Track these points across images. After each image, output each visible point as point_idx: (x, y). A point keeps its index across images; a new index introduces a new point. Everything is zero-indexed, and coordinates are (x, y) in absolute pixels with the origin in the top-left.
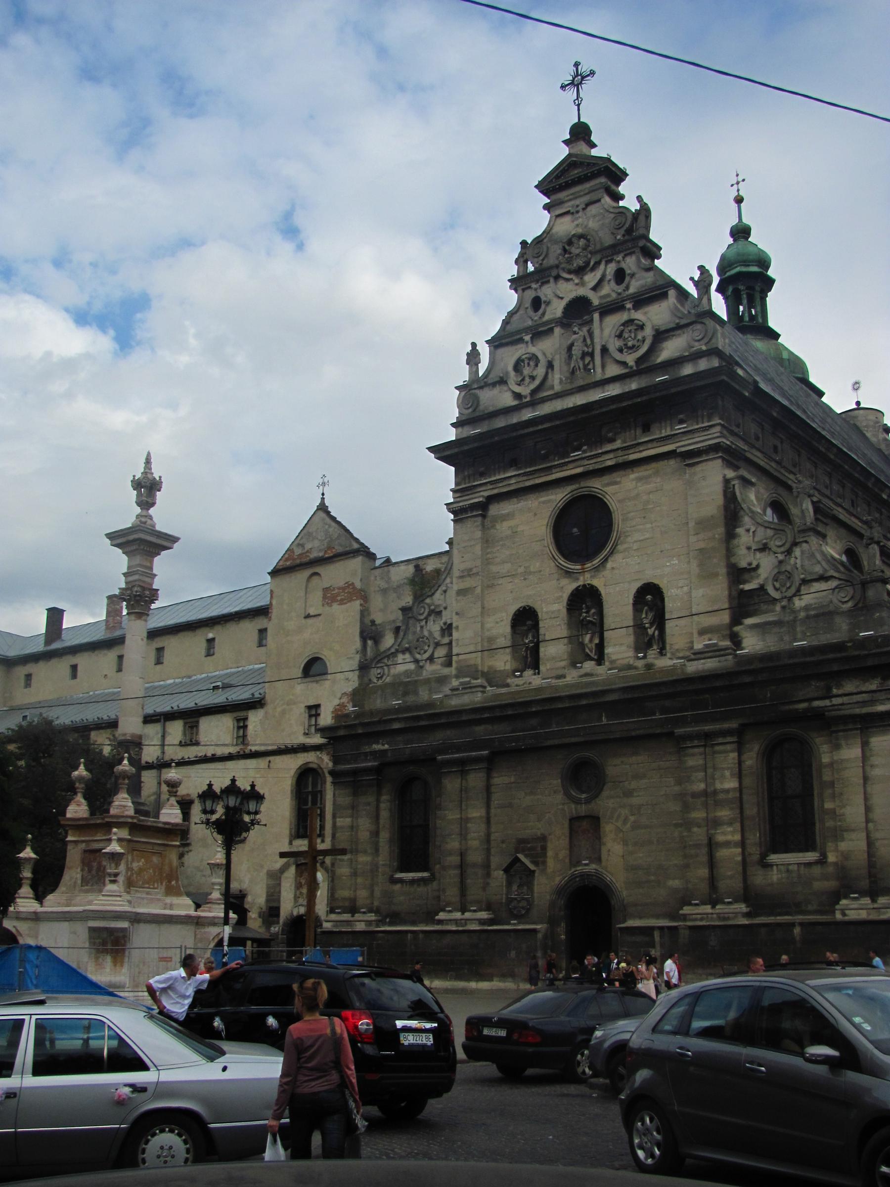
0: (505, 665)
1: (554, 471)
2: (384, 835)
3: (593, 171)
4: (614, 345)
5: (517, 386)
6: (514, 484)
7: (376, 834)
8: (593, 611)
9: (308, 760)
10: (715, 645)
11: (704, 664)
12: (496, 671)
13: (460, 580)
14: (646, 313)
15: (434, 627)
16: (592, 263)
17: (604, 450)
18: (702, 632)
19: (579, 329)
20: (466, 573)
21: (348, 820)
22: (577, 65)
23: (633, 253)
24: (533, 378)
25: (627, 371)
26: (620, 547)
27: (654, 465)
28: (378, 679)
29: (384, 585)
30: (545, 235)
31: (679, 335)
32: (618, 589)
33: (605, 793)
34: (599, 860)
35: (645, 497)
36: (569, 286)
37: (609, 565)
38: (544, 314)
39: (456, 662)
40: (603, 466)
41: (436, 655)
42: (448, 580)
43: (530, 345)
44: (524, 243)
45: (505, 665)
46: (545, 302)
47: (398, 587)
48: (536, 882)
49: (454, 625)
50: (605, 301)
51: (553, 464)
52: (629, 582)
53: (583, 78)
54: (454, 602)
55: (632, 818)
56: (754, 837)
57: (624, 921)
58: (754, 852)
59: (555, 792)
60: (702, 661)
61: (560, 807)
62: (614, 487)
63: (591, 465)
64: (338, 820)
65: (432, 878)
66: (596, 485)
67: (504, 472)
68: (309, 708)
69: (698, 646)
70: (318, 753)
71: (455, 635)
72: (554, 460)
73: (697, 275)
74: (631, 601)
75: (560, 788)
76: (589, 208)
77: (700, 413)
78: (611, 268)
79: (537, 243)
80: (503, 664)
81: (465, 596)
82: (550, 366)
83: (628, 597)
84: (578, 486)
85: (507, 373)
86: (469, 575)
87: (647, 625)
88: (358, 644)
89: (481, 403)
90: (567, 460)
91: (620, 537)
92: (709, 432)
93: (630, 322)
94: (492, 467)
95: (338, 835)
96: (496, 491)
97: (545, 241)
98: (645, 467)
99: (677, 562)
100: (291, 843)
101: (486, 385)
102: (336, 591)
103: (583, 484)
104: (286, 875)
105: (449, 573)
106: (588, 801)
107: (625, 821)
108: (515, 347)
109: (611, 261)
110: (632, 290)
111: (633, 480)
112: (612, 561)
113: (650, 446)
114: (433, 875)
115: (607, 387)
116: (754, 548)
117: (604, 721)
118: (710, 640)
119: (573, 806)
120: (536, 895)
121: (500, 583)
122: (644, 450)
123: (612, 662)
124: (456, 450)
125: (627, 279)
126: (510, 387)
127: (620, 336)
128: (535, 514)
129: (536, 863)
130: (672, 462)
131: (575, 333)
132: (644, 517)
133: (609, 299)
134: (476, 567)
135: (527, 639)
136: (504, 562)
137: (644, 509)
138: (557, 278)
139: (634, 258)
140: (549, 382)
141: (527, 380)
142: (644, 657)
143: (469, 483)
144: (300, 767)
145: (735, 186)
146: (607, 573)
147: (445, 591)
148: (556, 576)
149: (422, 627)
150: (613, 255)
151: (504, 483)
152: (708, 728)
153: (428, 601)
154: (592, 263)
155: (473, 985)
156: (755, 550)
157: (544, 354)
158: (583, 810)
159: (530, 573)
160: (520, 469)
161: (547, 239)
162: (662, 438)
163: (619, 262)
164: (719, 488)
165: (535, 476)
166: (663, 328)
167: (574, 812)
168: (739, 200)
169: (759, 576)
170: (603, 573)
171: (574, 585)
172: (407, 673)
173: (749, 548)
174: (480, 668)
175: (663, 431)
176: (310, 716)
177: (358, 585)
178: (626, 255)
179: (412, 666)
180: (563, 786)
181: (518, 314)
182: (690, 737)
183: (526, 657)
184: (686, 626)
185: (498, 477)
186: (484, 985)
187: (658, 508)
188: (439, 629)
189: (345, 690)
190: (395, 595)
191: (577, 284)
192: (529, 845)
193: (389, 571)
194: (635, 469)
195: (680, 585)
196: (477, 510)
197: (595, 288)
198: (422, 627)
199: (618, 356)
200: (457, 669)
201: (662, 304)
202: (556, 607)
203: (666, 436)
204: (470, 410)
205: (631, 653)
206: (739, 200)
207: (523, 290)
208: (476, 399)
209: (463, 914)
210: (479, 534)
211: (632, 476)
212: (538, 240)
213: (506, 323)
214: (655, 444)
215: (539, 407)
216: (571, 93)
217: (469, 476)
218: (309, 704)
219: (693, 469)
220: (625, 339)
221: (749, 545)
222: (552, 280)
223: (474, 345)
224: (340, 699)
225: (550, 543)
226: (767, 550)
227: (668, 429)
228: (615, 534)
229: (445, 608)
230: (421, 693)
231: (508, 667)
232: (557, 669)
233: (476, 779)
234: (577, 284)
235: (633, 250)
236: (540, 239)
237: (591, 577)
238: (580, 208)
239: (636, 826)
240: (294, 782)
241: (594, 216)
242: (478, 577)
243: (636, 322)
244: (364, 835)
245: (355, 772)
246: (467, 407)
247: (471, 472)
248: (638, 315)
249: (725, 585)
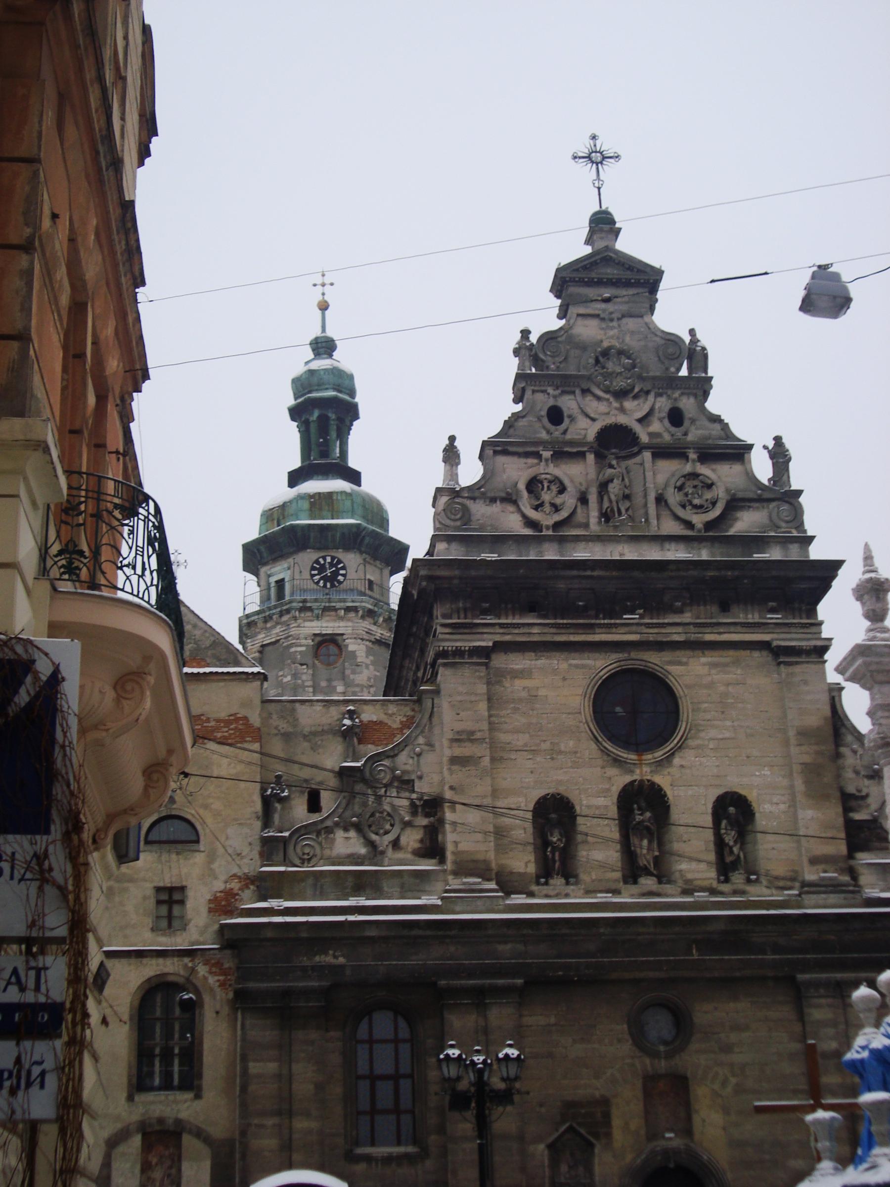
0: (526, 866)
1: (597, 630)
3: (639, 280)
4: (674, 499)
5: (533, 511)
6: (536, 634)
8: (648, 814)
9: (166, 970)
10: (830, 879)
11: (825, 899)
12: (512, 873)
13: (455, 744)
14: (713, 470)
16: (636, 390)
17: (671, 621)
18: (814, 861)
19: (617, 464)
20: (464, 737)
21: (272, 1067)
22: (594, 137)
23: (695, 396)
24: (556, 508)
25: (689, 533)
26: (690, 742)
27: (731, 653)
28: (303, 861)
29: (284, 726)
30: (562, 333)
31: (758, 508)
32: (690, 792)
33: (694, 1046)
34: (688, 1132)
35: (722, 688)
36: (602, 407)
37: (677, 761)
38: (565, 432)
39: (453, 853)
40: (668, 639)
41: (403, 840)
42: (421, 740)
43: (551, 465)
44: (525, 333)
45: (526, 866)
46: (570, 416)
47: (314, 734)
48: (596, 1160)
50: (655, 441)
51: (598, 621)
52: (706, 786)
53: (604, 158)
54: (446, 773)
55: (733, 1080)
59: (619, 1041)
60: (823, 896)
61: (628, 1061)
62: (677, 667)
63: (652, 635)
64: (251, 1065)
65: (425, 1153)
66: (654, 659)
67: (521, 617)
68: (158, 890)
69: (811, 875)
70: (186, 960)
71: (449, 816)
72: (597, 618)
73: (771, 444)
74: (710, 811)
75: (627, 1036)
76: (625, 321)
77: (796, 605)
78: (663, 404)
79: (552, 338)
80: (522, 865)
81: (464, 766)
82: (583, 500)
83: (705, 804)
84: (626, 655)
85: (518, 492)
86: (472, 741)
87: (731, 843)
88: (258, 806)
89: (472, 518)
90: (618, 621)
91: (690, 730)
92: (808, 631)
93: (694, 475)
94: (503, 606)
95: (252, 1088)
96: (507, 638)
97: (560, 339)
98: (721, 653)
99: (768, 773)
100: (130, 1098)
101: (483, 496)
102: (213, 724)
103: (633, 655)
104: (121, 1148)
105: (422, 732)
106: (669, 1056)
107: (724, 1083)
108: (523, 460)
109: (661, 395)
110: (690, 438)
111: (704, 665)
112: (681, 757)
113: (732, 629)
114: (425, 1153)
115: (667, 545)
116: (863, 773)
117: (695, 955)
118: (825, 872)
119: (648, 1061)
120: (597, 1179)
121: (513, 757)
122: (725, 633)
123: (688, 881)
124: (457, 573)
125: (686, 423)
126: (523, 508)
127: (680, 488)
128: (564, 679)
129: (597, 1136)
130: (756, 654)
131: (611, 466)
132: (723, 712)
133: (659, 440)
134: (480, 731)
135: (552, 835)
136: (517, 731)
137: (721, 702)
138: (586, 391)
139: (692, 400)
140: (580, 517)
141: (547, 508)
142: (727, 880)
143: (465, 618)
145: (319, 288)
146: (673, 770)
147: (419, 755)
148: (600, 762)
149: (378, 798)
150: (667, 389)
151: (522, 630)
152: (839, 976)
153: (386, 762)
154: (636, 390)
156: (863, 776)
157: (572, 481)
158: (662, 1065)
159: (560, 752)
160: (545, 617)
161: (564, 336)
162: (748, 623)
163: (676, 400)
164: (825, 698)
165: (572, 631)
166: (740, 495)
167: (649, 1068)
168: (324, 307)
169: (868, 806)
170: (669, 770)
171: (628, 779)
173: (857, 773)
174: (493, 865)
175: (750, 616)
176: (159, 902)
177: (255, 720)
178: (682, 394)
179: (363, 851)
180: (631, 1034)
181: (524, 420)
182: (817, 984)
183: (554, 861)
184: (785, 851)
185: (509, 621)
187: (740, 705)
189: (235, 870)
190: (306, 744)
191: (616, 409)
192: (583, 1111)
193: (294, 710)
194: (706, 652)
195: (775, 800)
196: (480, 657)
197: (640, 421)
198: (378, 798)
199: (681, 512)
200: (455, 862)
201: (733, 466)
202: (601, 801)
203: (755, 623)
204: (458, 523)
205: (712, 874)
206: (324, 307)
207: (534, 392)
208: (466, 510)
210: (482, 688)
211: (703, 660)
212: (548, 338)
213: (510, 424)
214: (739, 629)
215: (569, 546)
216: (587, 171)
217: (465, 610)
218: (161, 884)
219: (791, 669)
220: (686, 495)
221: (859, 768)
222: (578, 392)
223: (452, 439)
224: (226, 882)
225: (589, 719)
226: (877, 778)
227: (756, 615)
228: (684, 726)
229: (420, 778)
230: (386, 889)
231: (532, 869)
232: (608, 880)
234: (616, 409)
235: (694, 391)
236: (554, 336)
237: (651, 772)
238: (615, 316)
239: (739, 1090)
240: (136, 1003)
241: (633, 333)
242: (484, 745)
243: (701, 477)
244: (303, 1087)
245: (287, 993)
246: (453, 517)
247: (468, 605)
248: (704, 470)
249: (840, 810)
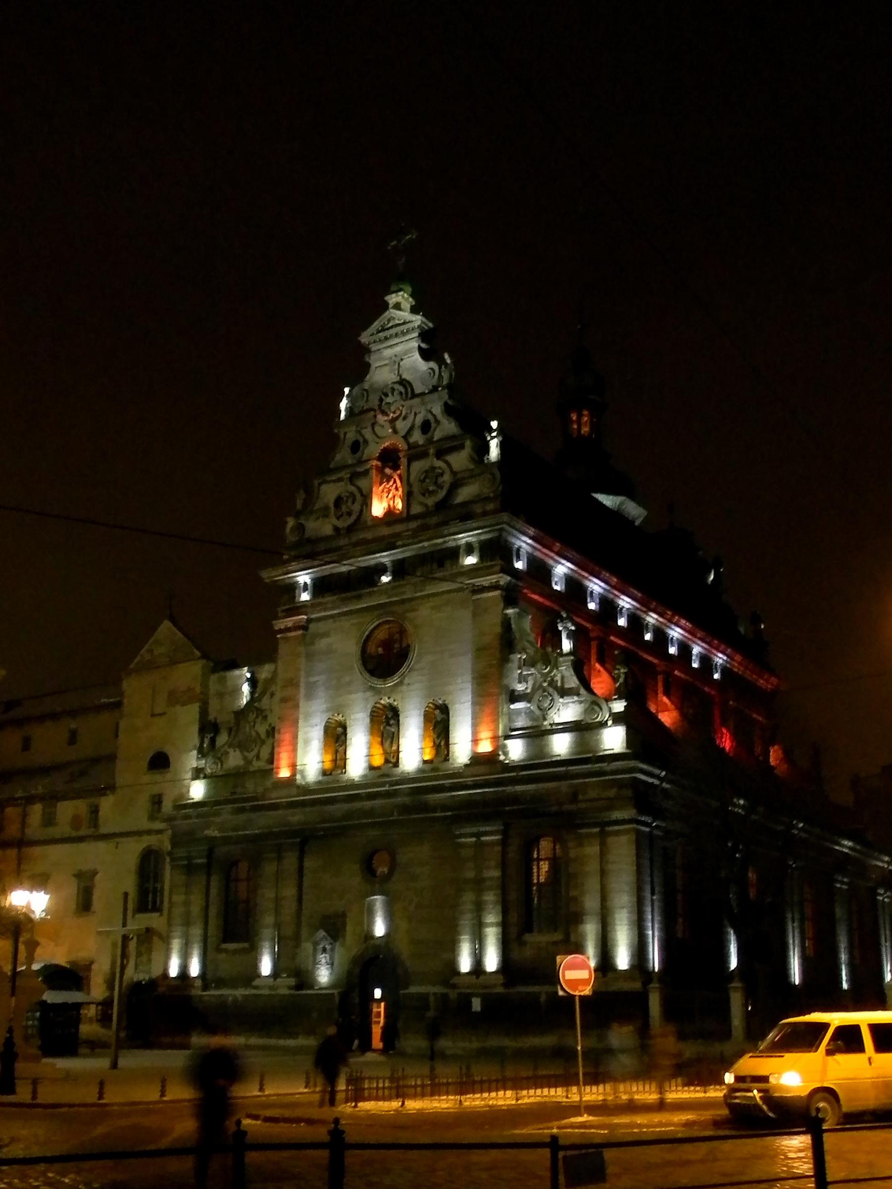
2: (213, 911)
7: (206, 908)
15: (262, 729)
37: (406, 681)
49: (276, 728)
56: (514, 918)
57: (407, 987)
58: (513, 931)
70: (160, 836)
144: (144, 849)
146: (404, 688)
155: (281, 1042)
172: (237, 768)
186: (291, 1042)
188: (265, 730)
209: (275, 979)
233: (290, 861)
